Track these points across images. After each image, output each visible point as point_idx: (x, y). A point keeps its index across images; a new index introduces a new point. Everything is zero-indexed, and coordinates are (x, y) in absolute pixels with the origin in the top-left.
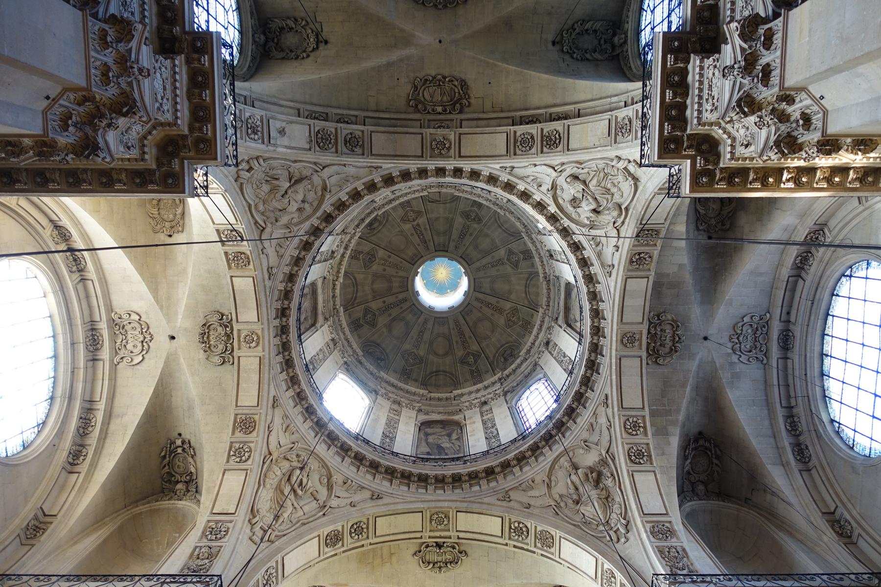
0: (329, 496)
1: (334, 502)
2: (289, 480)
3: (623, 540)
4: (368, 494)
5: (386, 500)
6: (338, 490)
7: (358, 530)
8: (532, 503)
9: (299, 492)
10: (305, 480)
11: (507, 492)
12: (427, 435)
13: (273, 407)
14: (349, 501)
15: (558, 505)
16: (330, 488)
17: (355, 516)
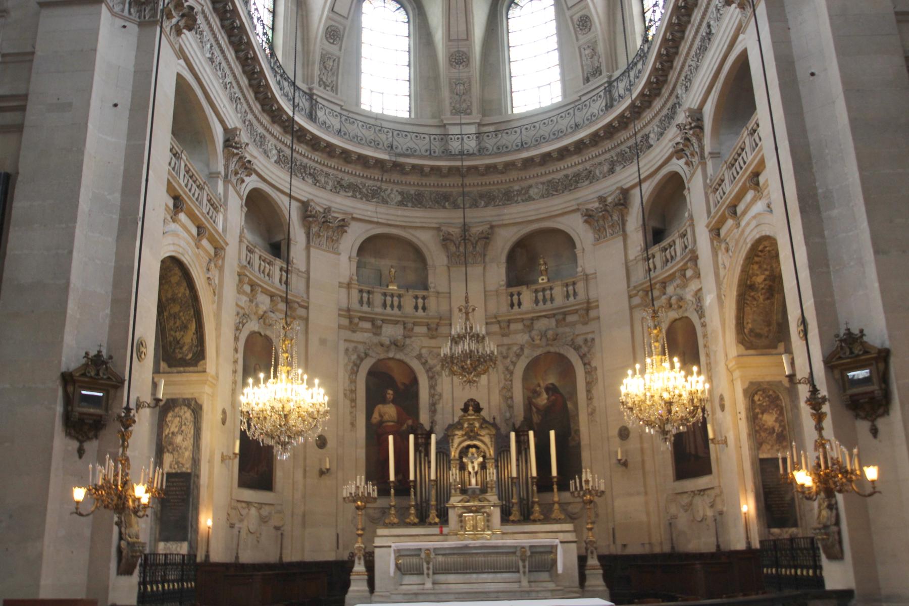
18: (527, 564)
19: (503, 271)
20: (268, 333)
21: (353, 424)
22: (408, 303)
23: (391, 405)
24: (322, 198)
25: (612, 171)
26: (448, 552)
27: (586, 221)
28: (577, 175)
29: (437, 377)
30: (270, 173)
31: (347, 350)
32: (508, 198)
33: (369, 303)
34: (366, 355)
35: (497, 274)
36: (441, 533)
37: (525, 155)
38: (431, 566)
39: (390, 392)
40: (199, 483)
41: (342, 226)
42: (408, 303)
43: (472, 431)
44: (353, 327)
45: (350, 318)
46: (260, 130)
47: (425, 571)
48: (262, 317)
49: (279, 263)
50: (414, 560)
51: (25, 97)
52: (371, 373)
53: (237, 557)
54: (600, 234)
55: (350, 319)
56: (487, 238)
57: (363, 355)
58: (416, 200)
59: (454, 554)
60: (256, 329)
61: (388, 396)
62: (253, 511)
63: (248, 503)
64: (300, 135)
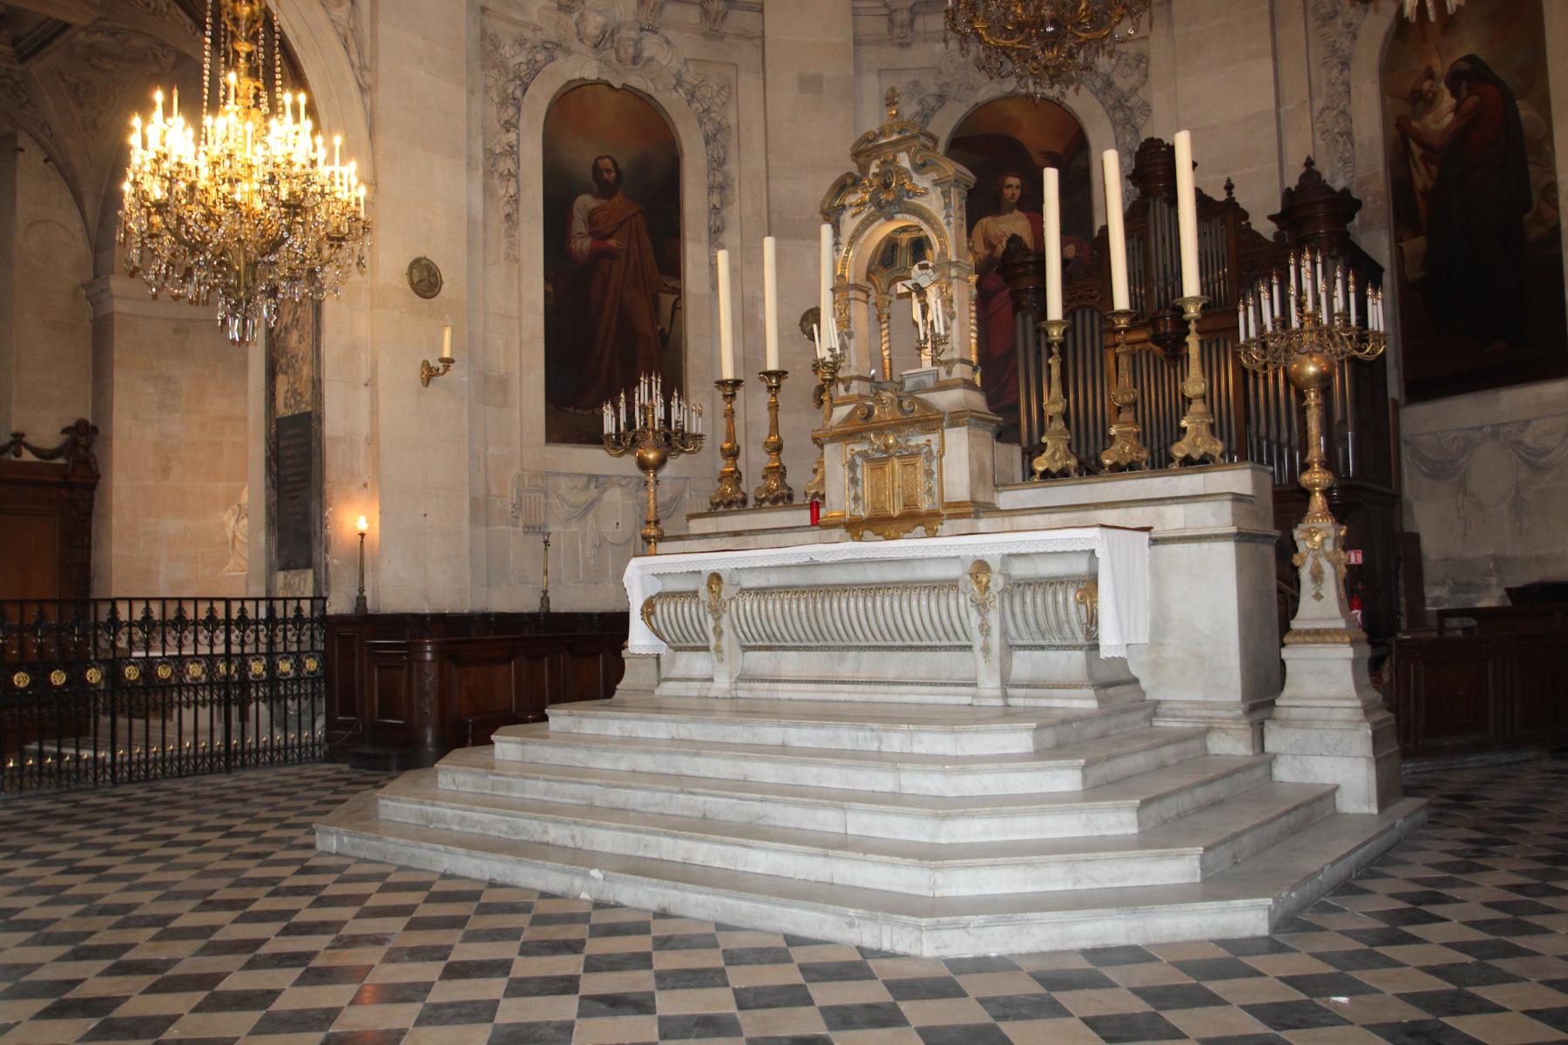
18: (994, 619)
20: (635, 81)
23: (1016, 213)
26: (775, 580)
29: (1139, 120)
34: (941, 99)
36: (815, 520)
38: (725, 623)
39: (1014, 181)
40: (321, 433)
43: (886, 186)
47: (713, 642)
50: (688, 608)
53: (545, 599)
57: (932, 101)
59: (786, 589)
60: (590, 72)
61: (1008, 192)
62: (614, 495)
63: (598, 481)
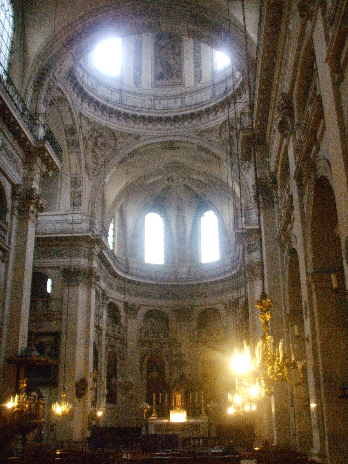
0: (116, 144)
1: (119, 146)
2: (97, 145)
3: (246, 171)
4: (133, 138)
5: (143, 138)
6: (120, 140)
7: (132, 154)
8: (213, 139)
9: (103, 148)
10: (103, 141)
11: (201, 132)
12: (160, 49)
13: (80, 117)
14: (125, 143)
15: (223, 144)
16: (115, 139)
17: (130, 150)
19: (196, 322)
21: (142, 379)
22: (162, 335)
24: (131, 300)
25: (233, 291)
27: (225, 308)
28: (222, 290)
30: (115, 295)
31: (140, 353)
32: (199, 295)
33: (148, 336)
35: (194, 324)
37: (204, 281)
41: (138, 309)
42: (162, 335)
44: (142, 345)
45: (141, 342)
46: (111, 282)
48: (113, 347)
49: (117, 326)
51: (61, 311)
52: (149, 361)
54: (229, 312)
55: (141, 343)
56: (190, 311)
58: (165, 296)
64: (124, 279)
